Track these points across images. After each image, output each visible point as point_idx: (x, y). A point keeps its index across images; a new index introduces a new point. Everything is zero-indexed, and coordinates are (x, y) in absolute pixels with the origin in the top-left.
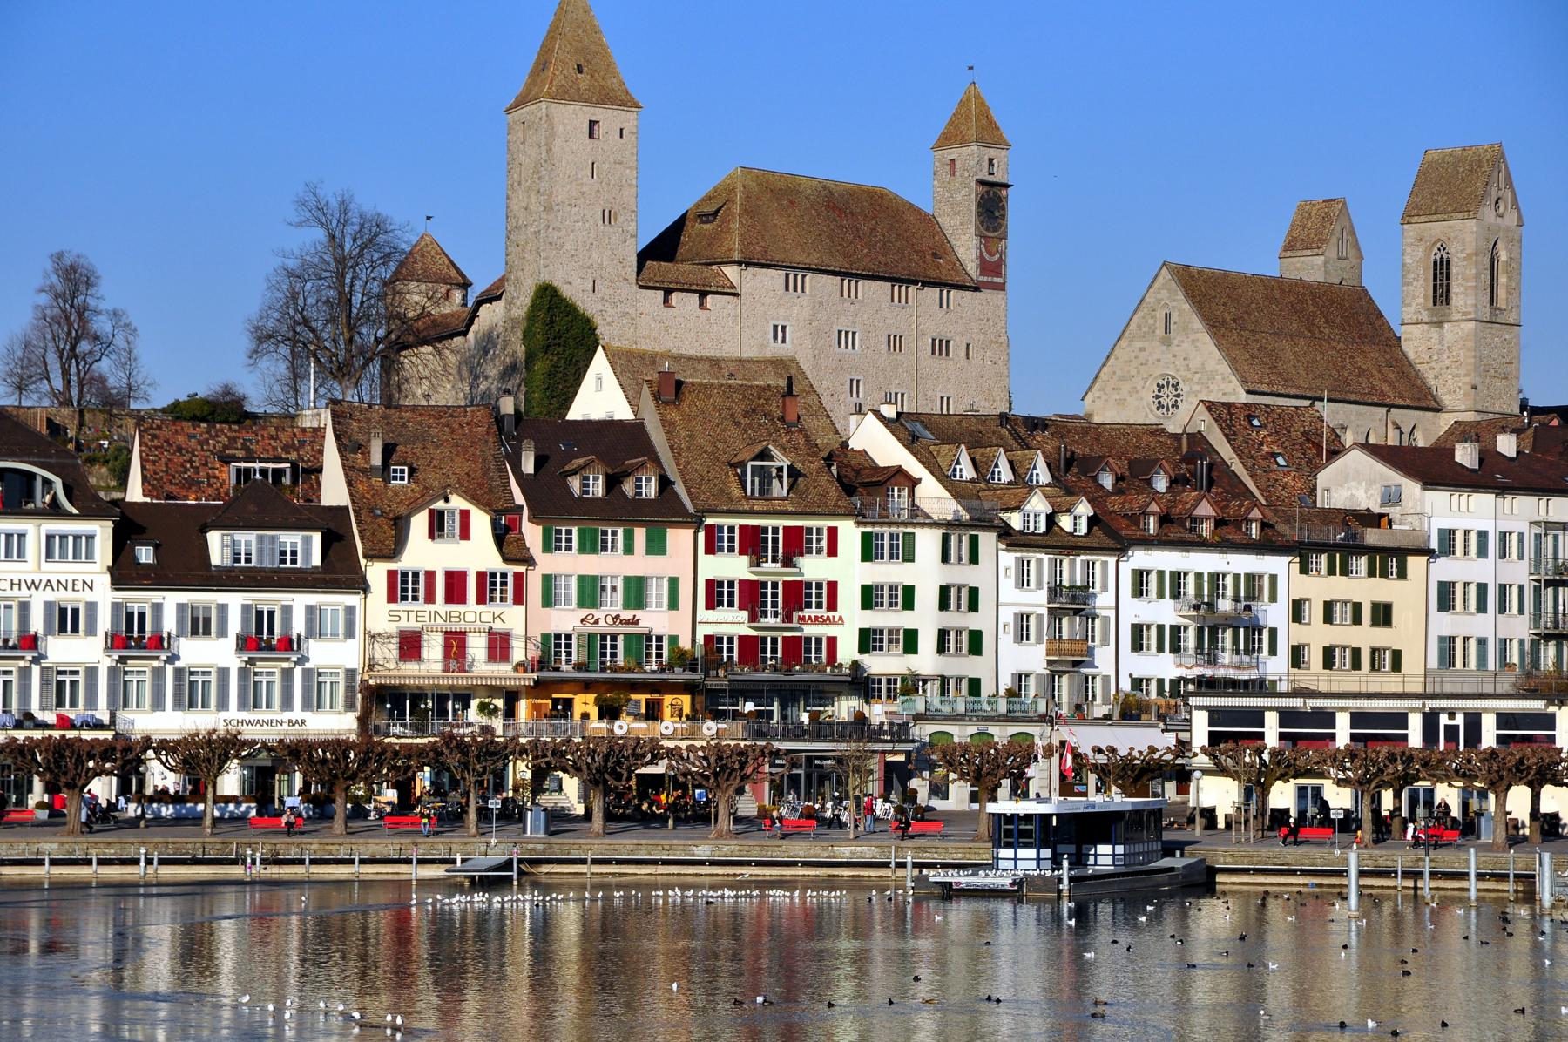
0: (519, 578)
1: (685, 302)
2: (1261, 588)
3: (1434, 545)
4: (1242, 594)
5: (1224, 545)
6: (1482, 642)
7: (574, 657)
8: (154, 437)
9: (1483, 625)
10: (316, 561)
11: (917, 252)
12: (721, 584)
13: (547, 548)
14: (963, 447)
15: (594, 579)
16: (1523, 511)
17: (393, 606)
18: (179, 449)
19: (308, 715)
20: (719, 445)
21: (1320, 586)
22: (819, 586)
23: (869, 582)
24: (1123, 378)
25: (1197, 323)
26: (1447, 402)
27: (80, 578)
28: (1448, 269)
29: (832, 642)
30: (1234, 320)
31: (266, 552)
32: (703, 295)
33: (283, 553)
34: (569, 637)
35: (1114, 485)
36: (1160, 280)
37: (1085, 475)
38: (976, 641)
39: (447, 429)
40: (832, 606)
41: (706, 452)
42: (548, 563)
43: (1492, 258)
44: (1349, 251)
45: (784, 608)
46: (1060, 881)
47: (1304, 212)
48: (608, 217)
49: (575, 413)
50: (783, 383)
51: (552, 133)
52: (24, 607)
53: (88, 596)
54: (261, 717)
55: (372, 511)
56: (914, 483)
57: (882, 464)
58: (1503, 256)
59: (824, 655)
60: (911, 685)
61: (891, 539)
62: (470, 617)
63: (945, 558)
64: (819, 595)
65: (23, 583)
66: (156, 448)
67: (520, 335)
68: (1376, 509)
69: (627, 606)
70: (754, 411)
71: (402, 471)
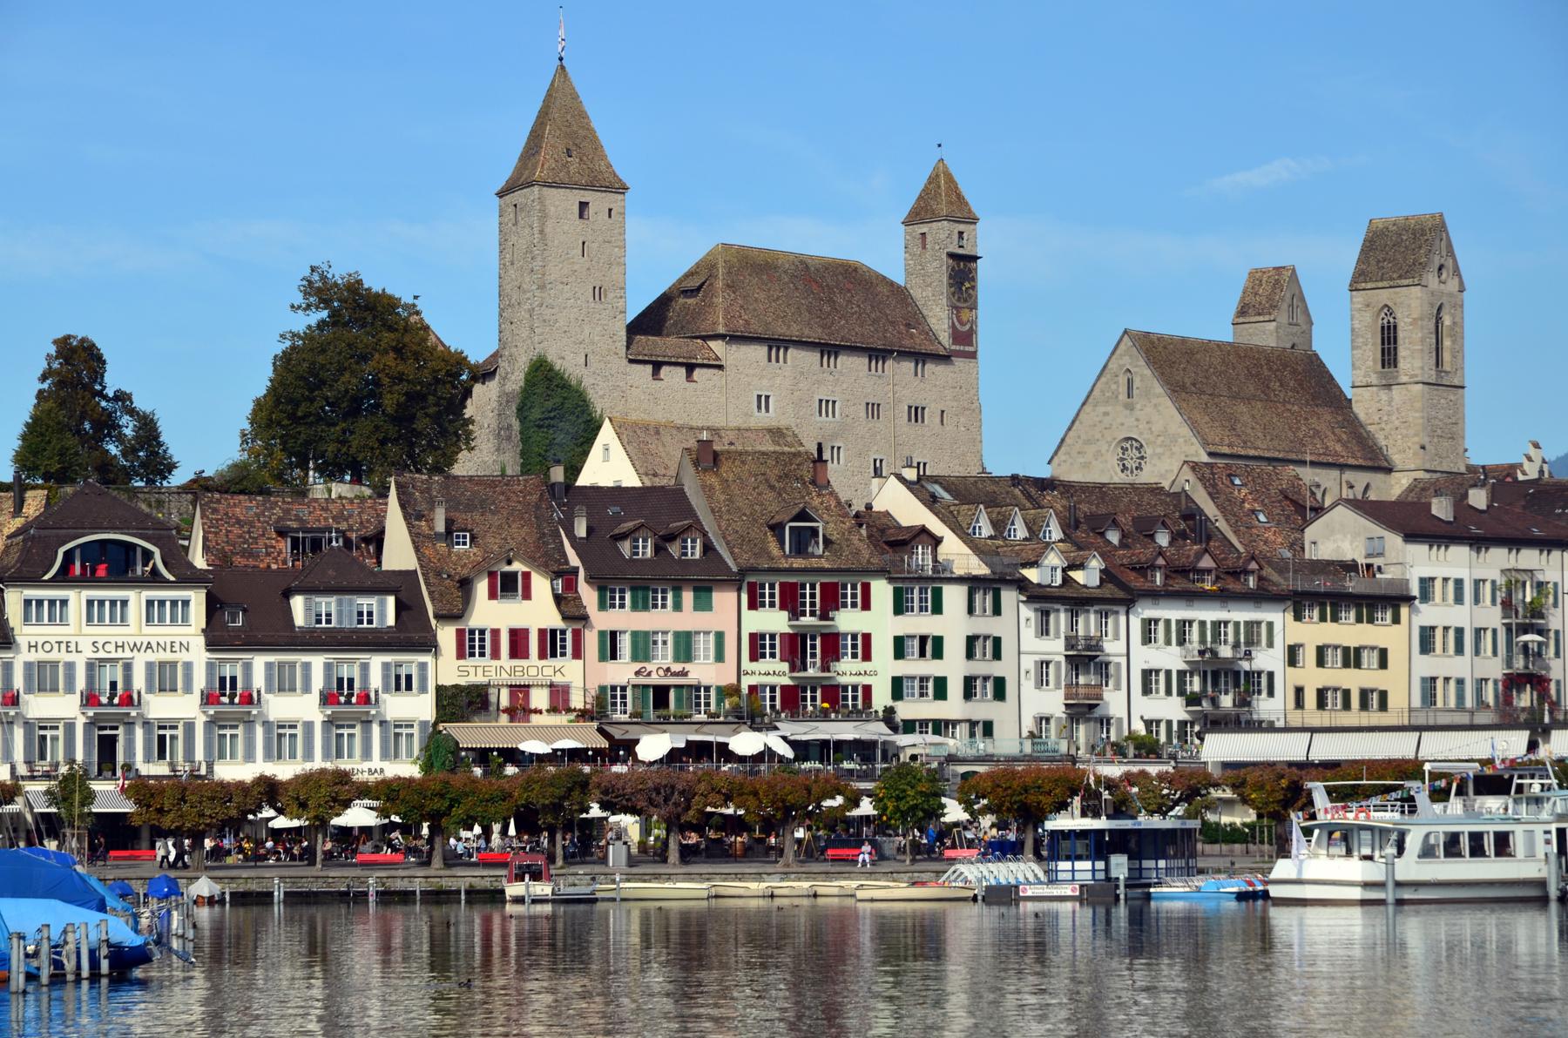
0: (577, 635)
1: (673, 376)
2: (1259, 634)
3: (1415, 590)
4: (1242, 640)
5: (1223, 597)
6: (1460, 682)
7: (629, 708)
8: (215, 511)
9: (1460, 667)
10: (391, 620)
11: (892, 323)
12: (763, 636)
13: (602, 606)
14: (981, 506)
15: (646, 634)
16: (1495, 562)
17: (462, 662)
18: (238, 521)
19: (386, 765)
20: (757, 507)
21: (1313, 632)
22: (854, 637)
23: (900, 633)
24: (1088, 442)
25: (1158, 389)
26: (1397, 462)
27: (177, 640)
28: (1395, 332)
29: (867, 690)
30: (1194, 385)
31: (345, 613)
32: (690, 368)
33: (360, 614)
34: (624, 689)
35: (1120, 541)
36: (1122, 347)
37: (1093, 530)
38: (1000, 691)
39: (502, 498)
40: (867, 656)
41: (745, 515)
42: (603, 620)
43: (1437, 322)
44: (1301, 319)
46: (1117, 887)
47: (1256, 277)
48: (598, 293)
49: (583, 480)
51: (544, 216)
52: (128, 667)
53: (182, 657)
55: (438, 574)
56: (937, 541)
57: (905, 523)
58: (1447, 321)
59: (860, 702)
60: (941, 727)
61: (921, 593)
62: (533, 671)
63: (971, 610)
64: (854, 646)
65: (126, 646)
66: (217, 520)
67: (514, 408)
68: (1362, 561)
69: (677, 659)
71: (465, 537)
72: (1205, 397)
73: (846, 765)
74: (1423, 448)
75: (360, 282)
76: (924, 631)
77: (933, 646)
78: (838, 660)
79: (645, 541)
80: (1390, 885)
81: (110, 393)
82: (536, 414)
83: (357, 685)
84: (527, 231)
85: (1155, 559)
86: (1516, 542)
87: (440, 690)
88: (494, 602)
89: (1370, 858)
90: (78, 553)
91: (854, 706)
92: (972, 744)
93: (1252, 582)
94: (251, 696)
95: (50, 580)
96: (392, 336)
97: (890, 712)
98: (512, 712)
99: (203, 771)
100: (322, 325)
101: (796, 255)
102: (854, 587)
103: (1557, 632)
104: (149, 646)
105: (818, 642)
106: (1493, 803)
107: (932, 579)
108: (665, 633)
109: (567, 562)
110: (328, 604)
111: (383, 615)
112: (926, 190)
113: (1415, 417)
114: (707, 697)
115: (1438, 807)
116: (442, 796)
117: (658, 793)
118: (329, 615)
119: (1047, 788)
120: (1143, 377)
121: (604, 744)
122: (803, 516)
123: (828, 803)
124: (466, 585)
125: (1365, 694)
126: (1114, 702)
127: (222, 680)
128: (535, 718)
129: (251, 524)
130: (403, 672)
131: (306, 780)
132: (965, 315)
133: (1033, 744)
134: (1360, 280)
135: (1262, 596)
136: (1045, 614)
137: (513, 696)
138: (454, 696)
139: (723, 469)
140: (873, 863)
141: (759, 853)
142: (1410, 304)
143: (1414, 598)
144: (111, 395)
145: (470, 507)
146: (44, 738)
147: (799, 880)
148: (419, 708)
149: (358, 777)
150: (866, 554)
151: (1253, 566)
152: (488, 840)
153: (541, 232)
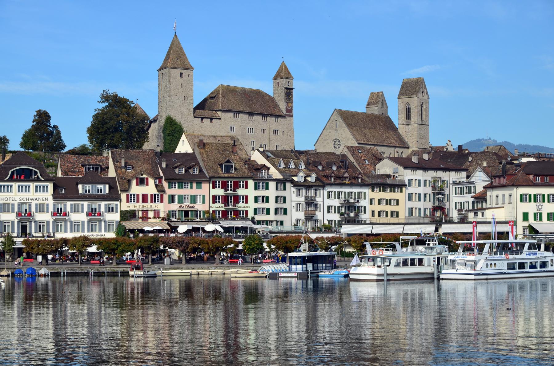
0: (162, 196)
2: (361, 196)
3: (407, 183)
5: (351, 185)
6: (420, 209)
7: (177, 217)
8: (64, 159)
10: (107, 192)
12: (216, 196)
13: (169, 188)
15: (182, 196)
16: (430, 175)
17: (128, 204)
18: (71, 162)
19: (106, 233)
20: (216, 159)
21: (377, 195)
23: (256, 195)
24: (325, 140)
25: (344, 125)
27: (44, 197)
29: (247, 212)
31: (94, 189)
32: (212, 119)
33: (98, 190)
34: (175, 211)
36: (334, 114)
37: (314, 166)
38: (285, 212)
40: (247, 202)
42: (169, 192)
45: (234, 203)
46: (308, 273)
47: (372, 95)
48: (185, 98)
49: (177, 151)
50: (233, 142)
51: (170, 77)
52: (30, 205)
53: (46, 202)
54: (93, 234)
55: (122, 178)
56: (268, 169)
57: (260, 164)
58: (424, 107)
59: (245, 215)
60: (268, 223)
62: (149, 206)
63: (277, 189)
64: (243, 199)
68: (392, 174)
69: (191, 203)
70: (225, 150)
72: (357, 128)
73: (239, 234)
74: (418, 142)
75: (117, 95)
76: (263, 195)
77: (266, 199)
78: (238, 203)
79: (182, 169)
80: (385, 275)
81: (52, 126)
82: (167, 132)
83: (97, 210)
84: (165, 81)
85: (332, 174)
86: (436, 169)
87: (121, 212)
88: (137, 186)
89: (379, 267)
90: (15, 172)
91: (243, 216)
92: (277, 228)
93: (360, 181)
94: (66, 213)
95: (7, 180)
96: (125, 110)
97: (253, 218)
98: (142, 218)
99: (52, 235)
100: (107, 107)
101: (242, 88)
102: (243, 182)
103: (448, 195)
104: (36, 199)
105: (232, 198)
106: (421, 248)
107: (266, 180)
108: (188, 195)
109: (160, 175)
110: (89, 187)
111: (105, 190)
112: (279, 70)
113: (415, 133)
114: (200, 214)
115: (404, 249)
116: (115, 244)
117: (179, 243)
118: (89, 190)
119: (293, 242)
120: (340, 122)
121: (169, 228)
122: (228, 161)
123: (229, 246)
124: (129, 181)
125: (392, 213)
126: (319, 215)
127: (58, 209)
128: (149, 220)
129: (74, 163)
130: (111, 207)
131: (76, 239)
132: (290, 105)
133: (294, 227)
134: (401, 95)
135: (363, 185)
136: (299, 190)
137: (143, 214)
138: (125, 214)
139: (206, 148)
140: (242, 263)
141: (211, 260)
142: (414, 102)
143: (407, 185)
144: (52, 126)
145: (132, 159)
146: (5, 226)
147: (220, 269)
148: (116, 217)
149: (92, 238)
150: (247, 172)
151: (360, 176)
152: (133, 256)
153: (169, 81)
